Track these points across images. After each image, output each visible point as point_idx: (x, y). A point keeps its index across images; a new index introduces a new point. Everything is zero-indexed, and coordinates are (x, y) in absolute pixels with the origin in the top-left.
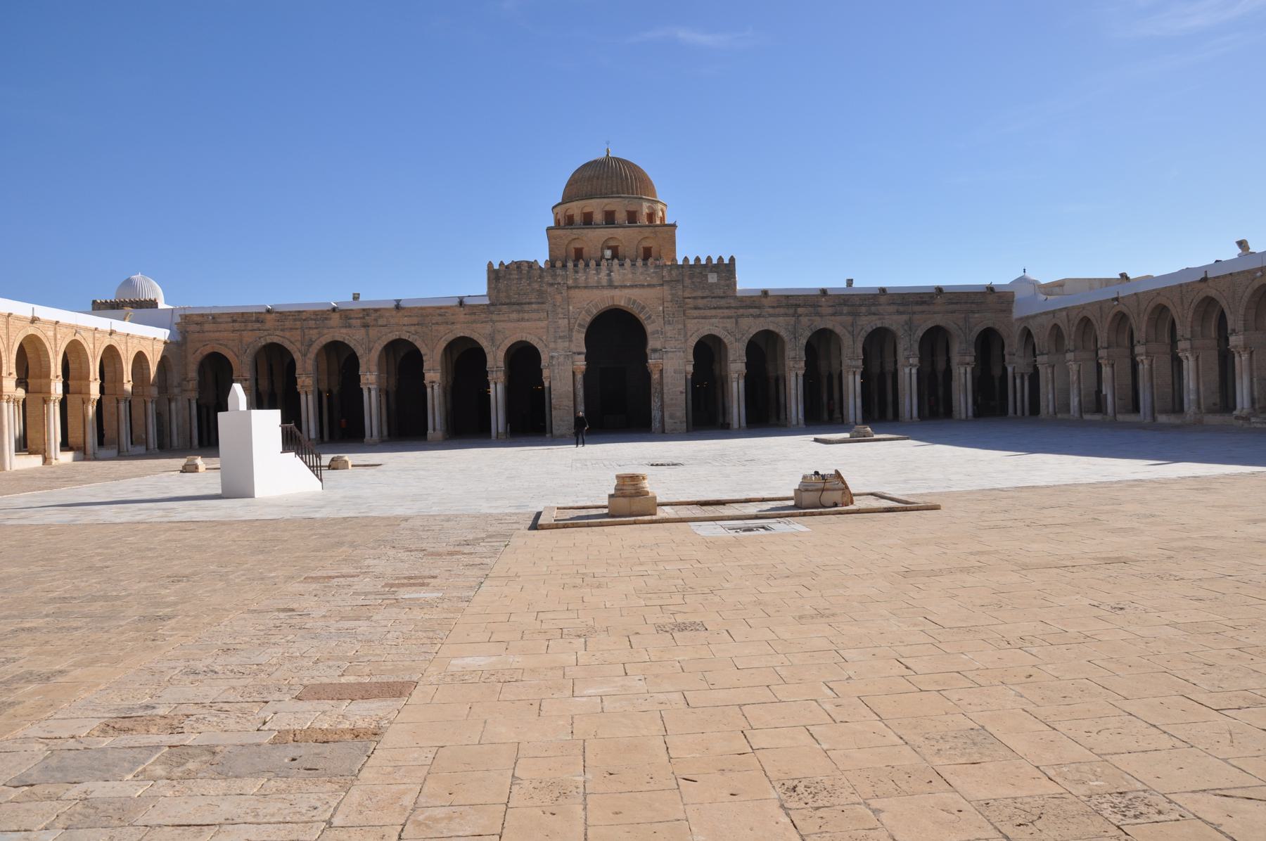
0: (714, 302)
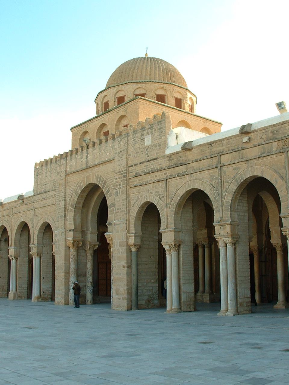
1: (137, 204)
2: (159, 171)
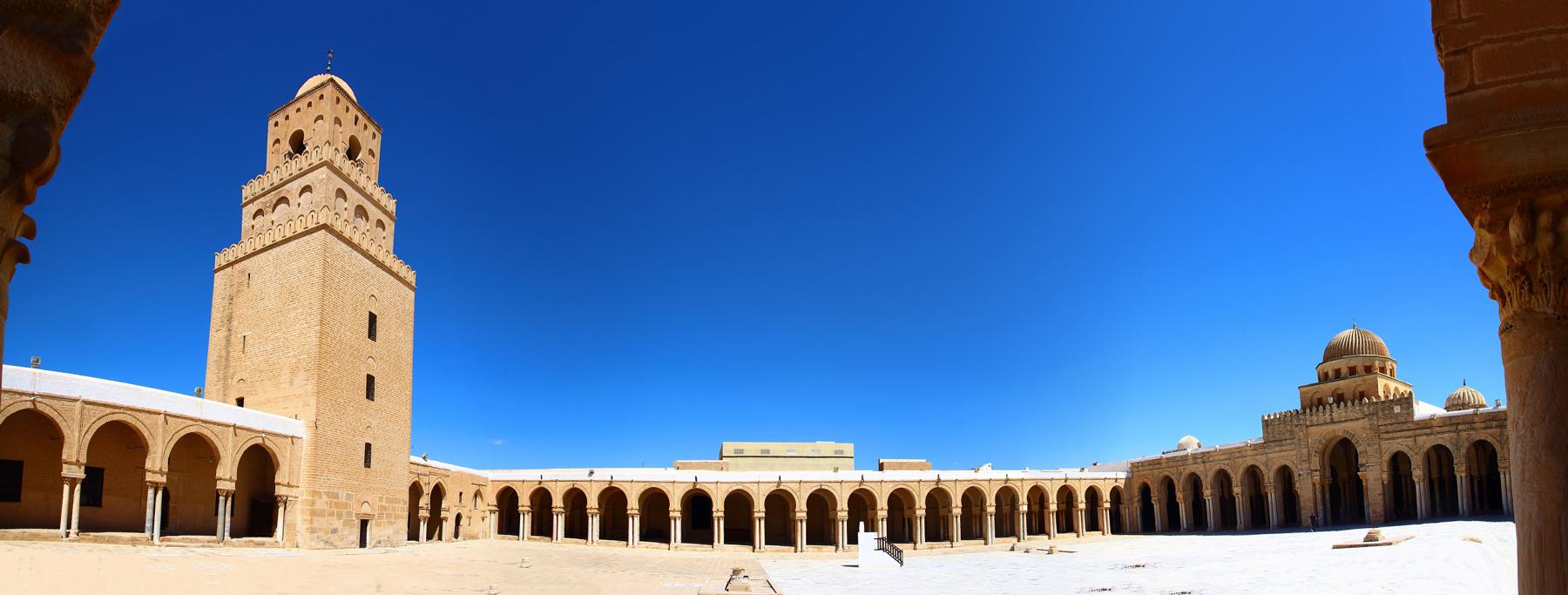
0: (1399, 427)
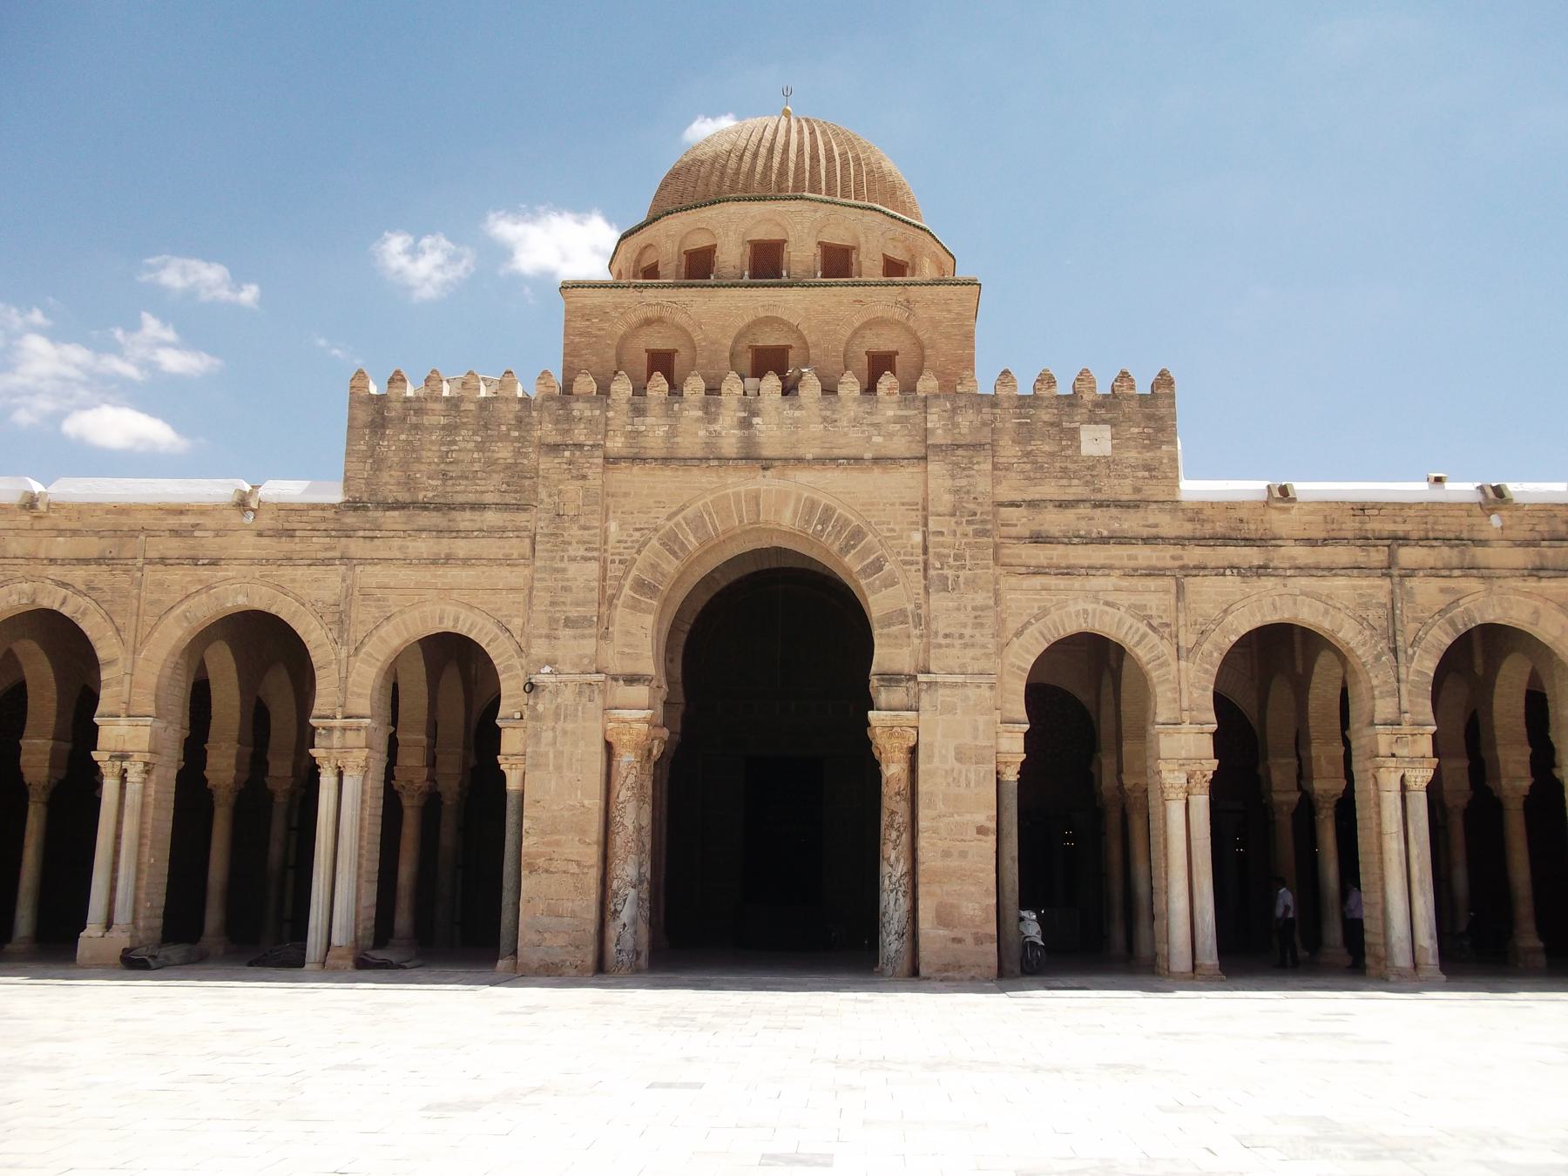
0: (1103, 521)
1: (1041, 633)
2: (1147, 541)
